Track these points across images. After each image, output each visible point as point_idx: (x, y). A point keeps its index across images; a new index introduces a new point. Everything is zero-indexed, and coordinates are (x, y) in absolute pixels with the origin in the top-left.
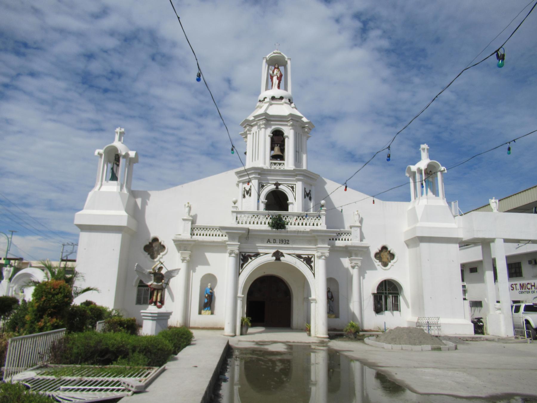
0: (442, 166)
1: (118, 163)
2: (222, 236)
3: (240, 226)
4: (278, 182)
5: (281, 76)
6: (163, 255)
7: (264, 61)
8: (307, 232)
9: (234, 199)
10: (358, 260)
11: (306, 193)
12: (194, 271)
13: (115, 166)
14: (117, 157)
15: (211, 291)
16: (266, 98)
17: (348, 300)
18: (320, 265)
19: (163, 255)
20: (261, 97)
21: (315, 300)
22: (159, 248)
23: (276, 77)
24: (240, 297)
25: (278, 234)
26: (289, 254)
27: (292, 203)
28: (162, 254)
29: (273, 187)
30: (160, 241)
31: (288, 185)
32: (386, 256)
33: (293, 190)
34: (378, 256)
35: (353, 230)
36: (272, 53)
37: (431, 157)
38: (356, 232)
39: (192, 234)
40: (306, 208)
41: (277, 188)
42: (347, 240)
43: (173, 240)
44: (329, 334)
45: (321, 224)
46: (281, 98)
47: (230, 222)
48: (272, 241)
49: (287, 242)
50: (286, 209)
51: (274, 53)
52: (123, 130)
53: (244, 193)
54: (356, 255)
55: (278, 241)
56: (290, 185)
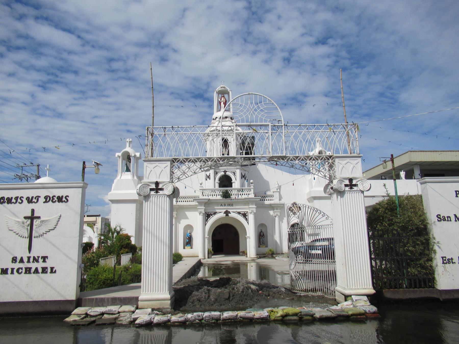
1: (129, 161)
3: (205, 197)
5: (226, 101)
7: (215, 92)
8: (243, 199)
9: (201, 182)
10: (278, 212)
12: (180, 223)
13: (128, 162)
17: (273, 236)
18: (251, 217)
20: (214, 117)
21: (249, 237)
24: (206, 237)
25: (227, 201)
26: (233, 212)
27: (234, 182)
29: (223, 173)
35: (274, 194)
36: (220, 87)
38: (276, 195)
39: (177, 201)
40: (242, 185)
41: (225, 173)
42: (271, 200)
48: (223, 205)
49: (232, 205)
50: (232, 187)
51: (221, 88)
52: (131, 140)
53: (206, 178)
54: (277, 209)
55: (227, 205)
56: (233, 172)
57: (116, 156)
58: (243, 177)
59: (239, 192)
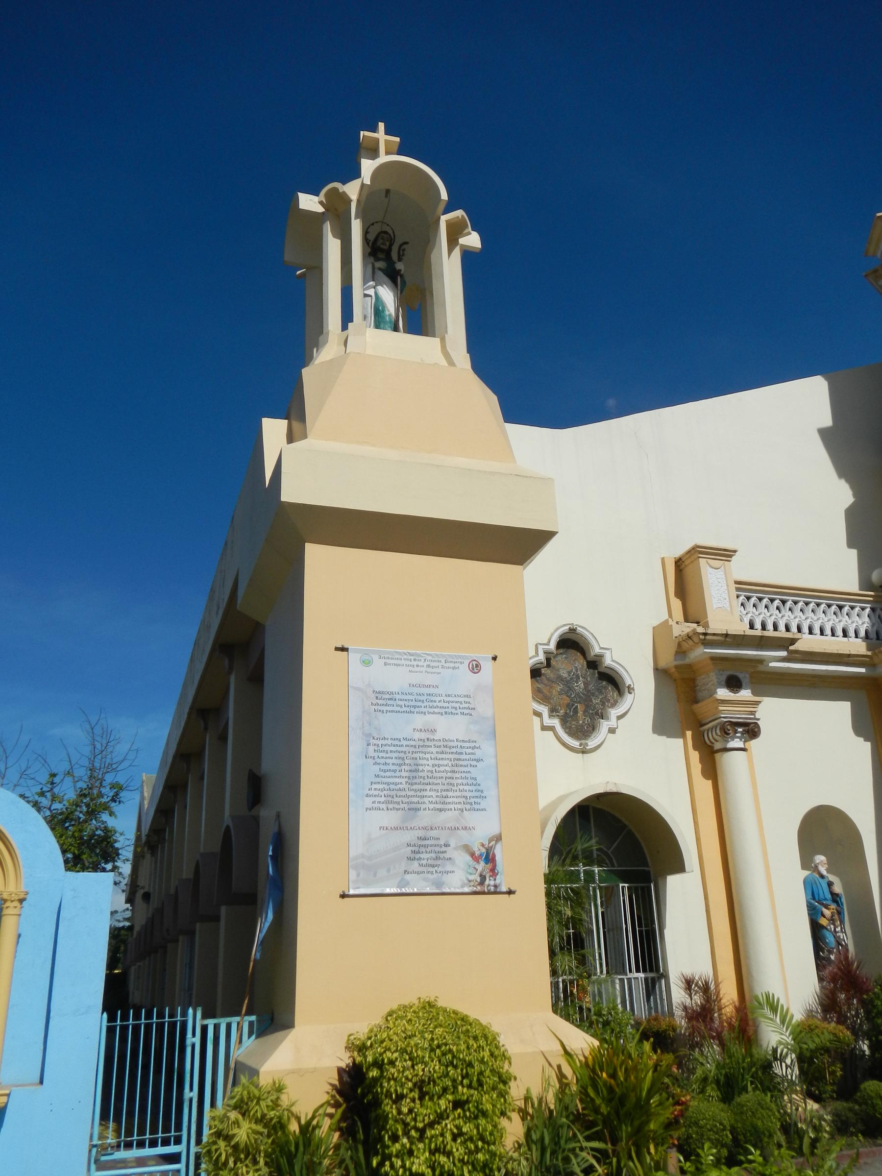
6: (620, 717)
14: (388, 243)
19: (620, 717)
28: (614, 713)
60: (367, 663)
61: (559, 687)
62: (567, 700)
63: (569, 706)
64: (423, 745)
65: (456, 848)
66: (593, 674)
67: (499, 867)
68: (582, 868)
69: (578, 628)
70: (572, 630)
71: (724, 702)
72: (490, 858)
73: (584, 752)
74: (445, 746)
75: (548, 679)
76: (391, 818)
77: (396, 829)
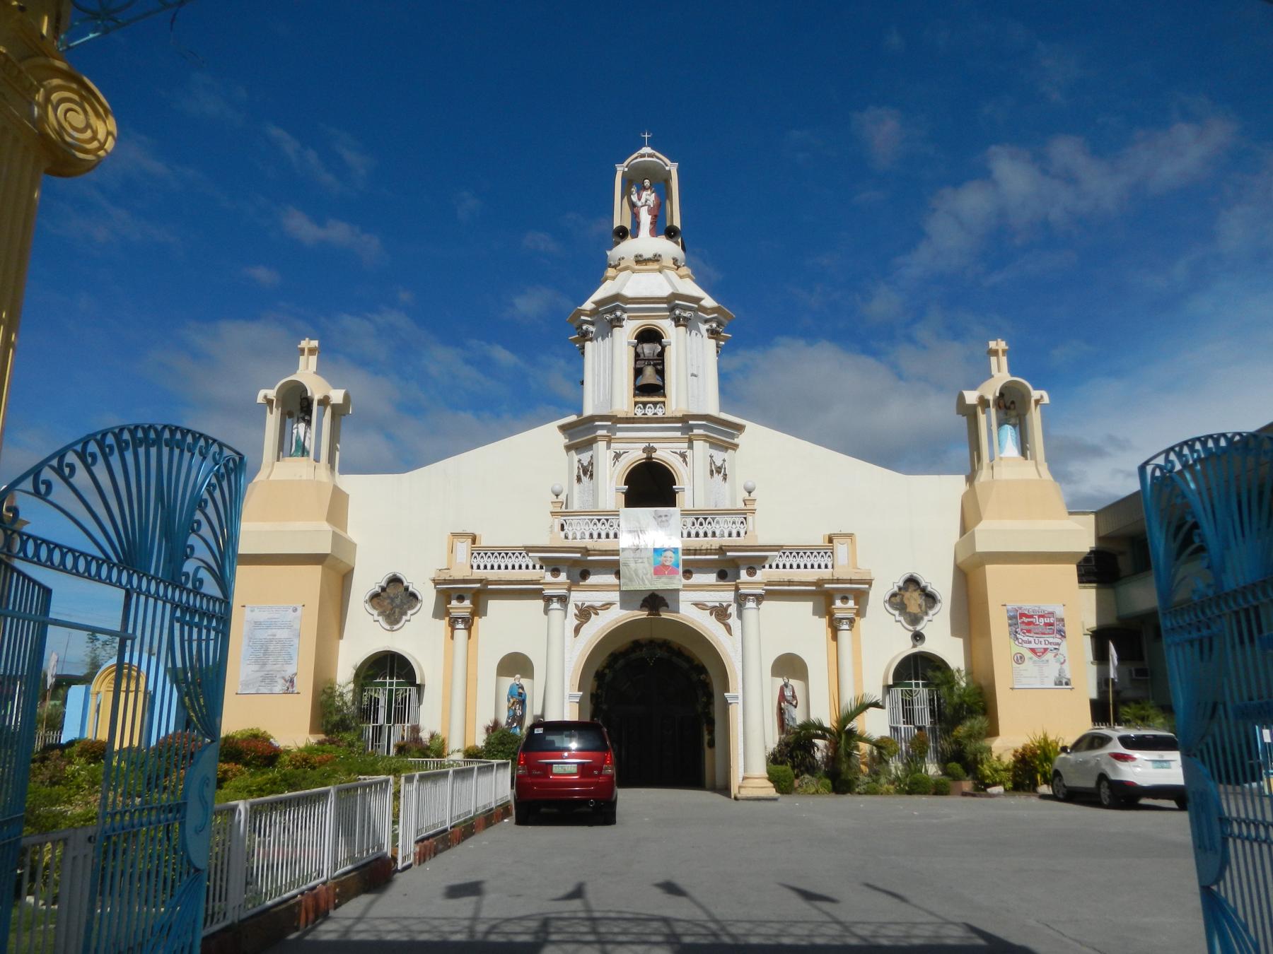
0: (1036, 388)
2: (534, 567)
3: (570, 543)
4: (651, 445)
6: (412, 615)
9: (557, 488)
11: (715, 465)
14: (306, 404)
15: (521, 691)
16: (623, 258)
19: (412, 615)
22: (405, 601)
23: (647, 207)
28: (410, 612)
30: (405, 584)
31: (672, 450)
32: (915, 600)
33: (685, 460)
34: (898, 599)
37: (1012, 371)
43: (434, 580)
44: (768, 772)
45: (746, 533)
46: (656, 259)
47: (544, 533)
51: (643, 156)
53: (579, 472)
57: (260, 399)
58: (719, 470)
59: (701, 524)
60: (252, 611)
61: (388, 601)
62: (390, 607)
63: (392, 610)
64: (271, 641)
65: (279, 678)
66: (406, 594)
67: (295, 684)
68: (388, 680)
69: (398, 575)
70: (394, 575)
71: (451, 608)
72: (292, 681)
73: (393, 631)
74: (280, 641)
75: (385, 598)
76: (256, 667)
77: (257, 671)
